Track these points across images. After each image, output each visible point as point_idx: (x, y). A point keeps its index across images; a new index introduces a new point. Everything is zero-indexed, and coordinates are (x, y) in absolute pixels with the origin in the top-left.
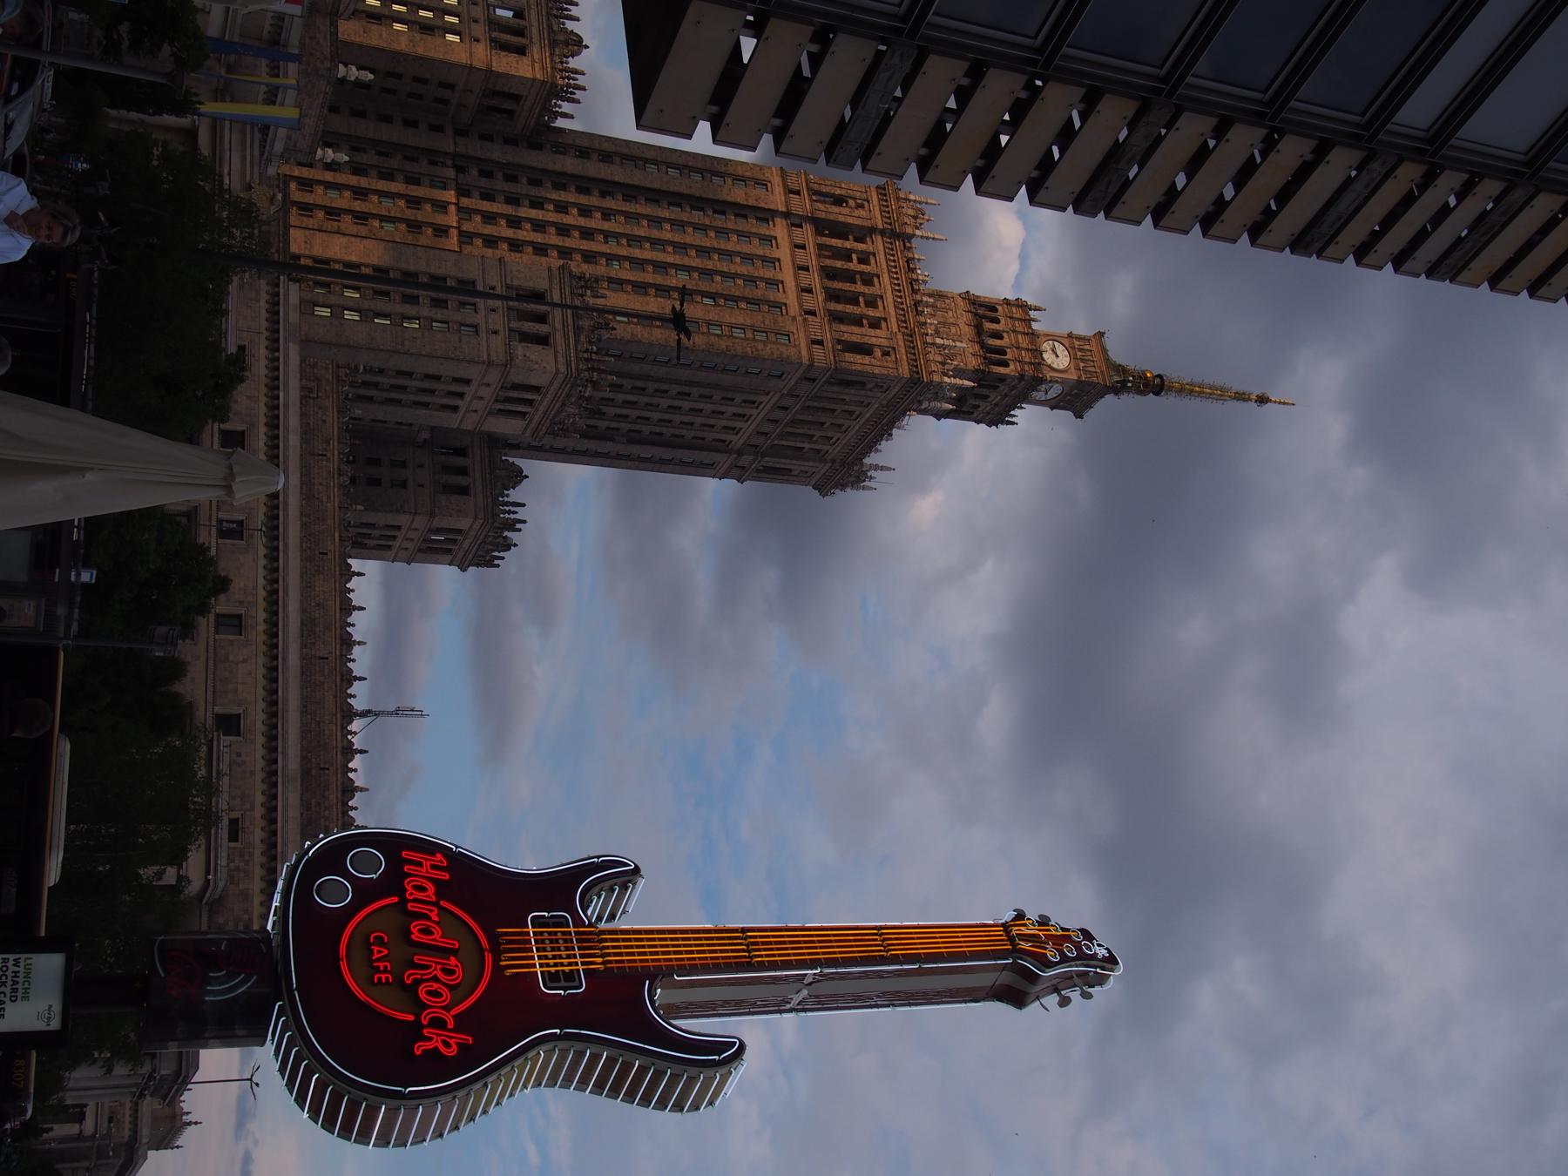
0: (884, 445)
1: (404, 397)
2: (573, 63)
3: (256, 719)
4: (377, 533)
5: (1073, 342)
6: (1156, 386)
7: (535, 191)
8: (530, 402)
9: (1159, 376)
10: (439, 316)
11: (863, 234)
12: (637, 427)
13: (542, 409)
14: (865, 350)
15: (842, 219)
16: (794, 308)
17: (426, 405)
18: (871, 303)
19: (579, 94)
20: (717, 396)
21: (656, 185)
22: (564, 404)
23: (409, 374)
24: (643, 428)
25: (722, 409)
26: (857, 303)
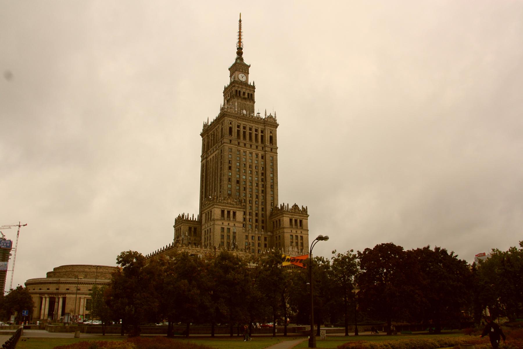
4: (294, 241)
5: (231, 76)
8: (229, 212)
16: (217, 152)
17: (234, 237)
19: (186, 214)
22: (228, 203)
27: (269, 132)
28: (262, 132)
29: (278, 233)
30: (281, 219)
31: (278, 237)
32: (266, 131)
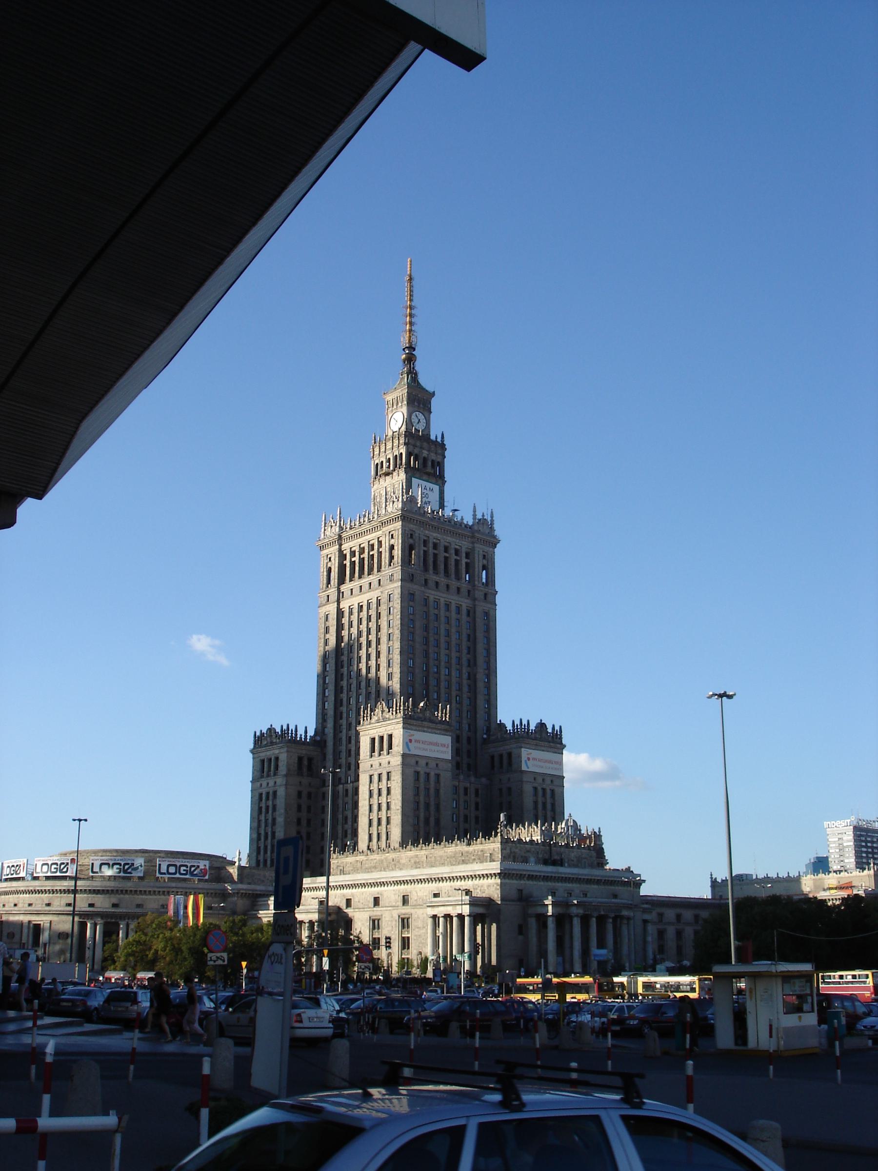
1: (432, 803)
3: (434, 887)
6: (411, 348)
7: (344, 742)
11: (342, 556)
17: (437, 791)
18: (372, 547)
19: (292, 727)
22: (425, 720)
25: (443, 619)
26: (373, 555)
28: (467, 555)
32: (476, 555)
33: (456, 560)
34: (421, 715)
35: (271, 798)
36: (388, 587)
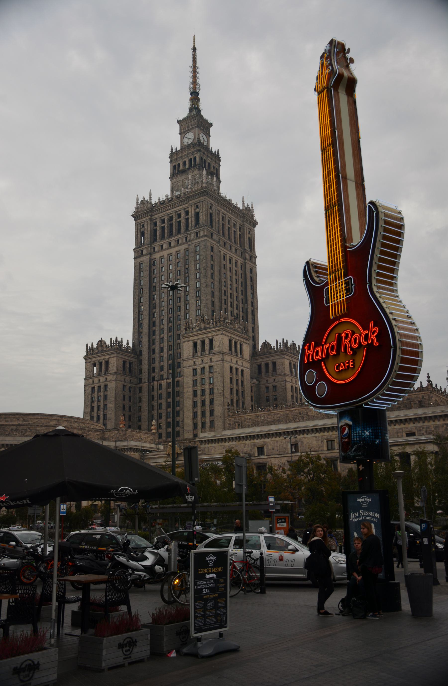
0: (234, 202)
1: (240, 390)
2: (108, 343)
4: (295, 395)
5: (182, 133)
7: (157, 351)
8: (236, 343)
9: (191, 94)
10: (208, 381)
12: (241, 301)
13: (237, 338)
14: (197, 215)
15: (149, 232)
16: (186, 246)
17: (242, 382)
18: (179, 216)
19: (119, 339)
20: (223, 271)
21: (147, 306)
22: (235, 330)
23: (232, 389)
24: (240, 298)
27: (248, 231)
29: (271, 380)
30: (279, 362)
31: (271, 388)
32: (245, 230)
33: (234, 231)
34: (232, 326)
35: (102, 390)
36: (195, 241)
